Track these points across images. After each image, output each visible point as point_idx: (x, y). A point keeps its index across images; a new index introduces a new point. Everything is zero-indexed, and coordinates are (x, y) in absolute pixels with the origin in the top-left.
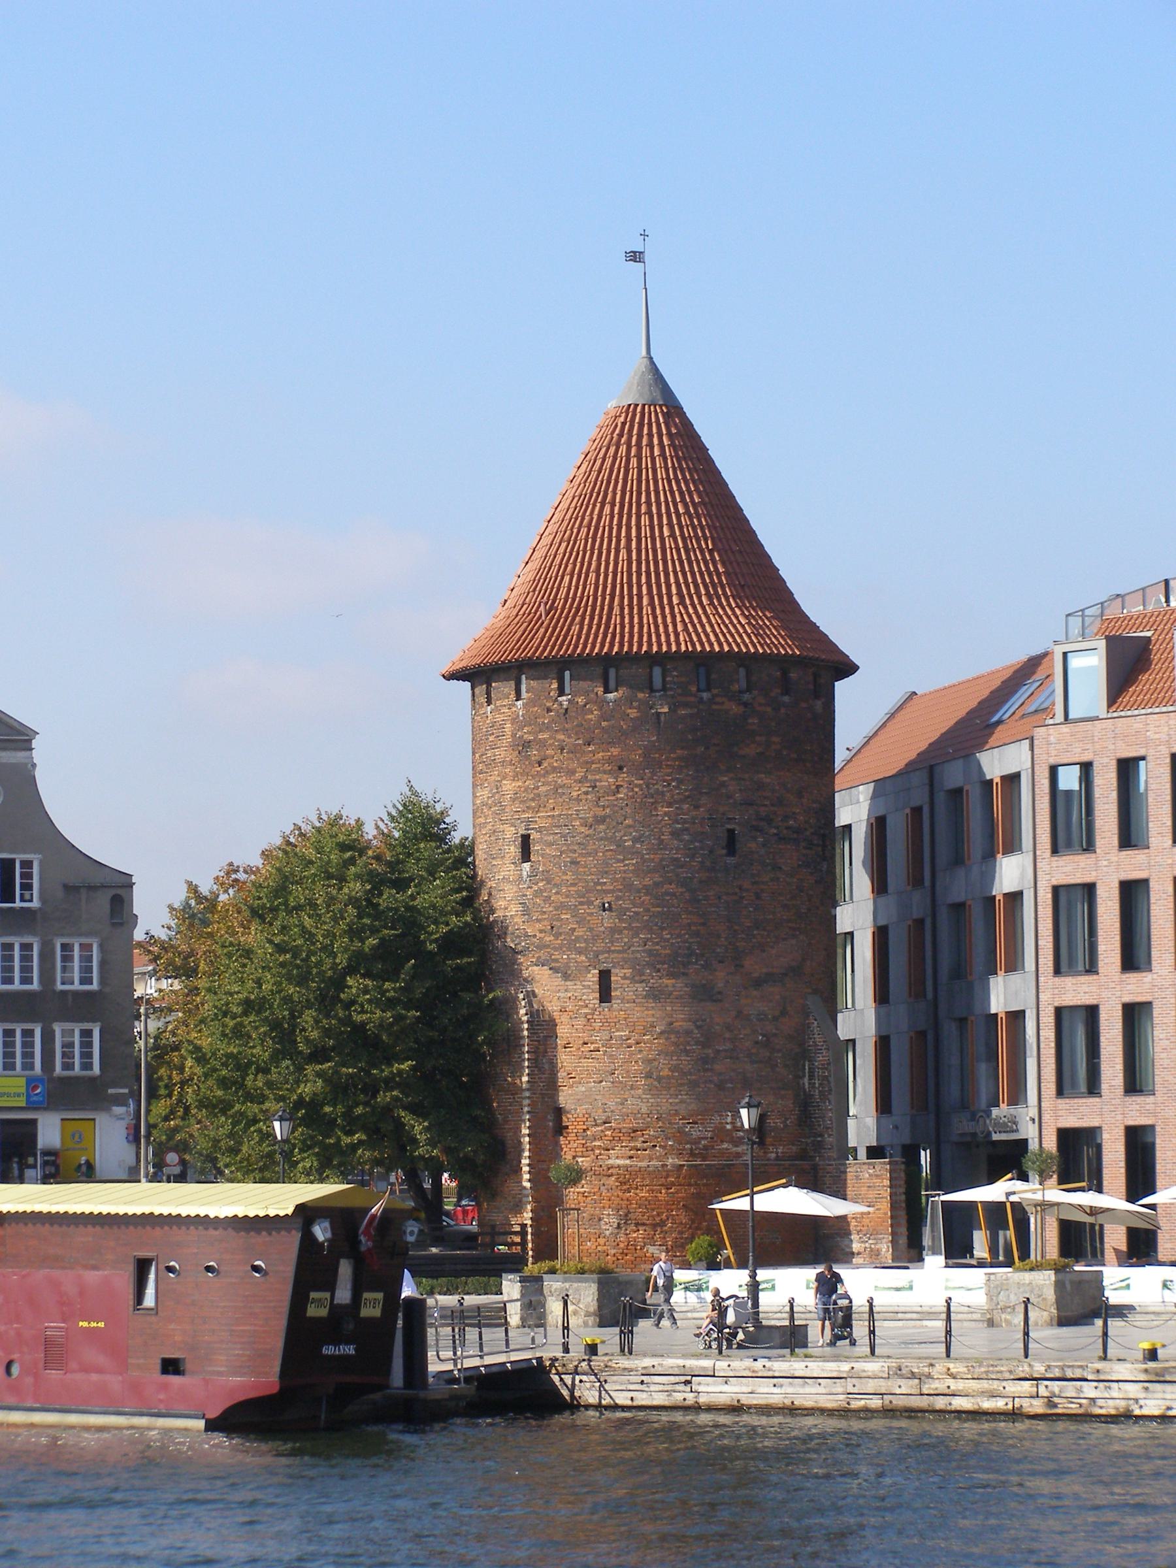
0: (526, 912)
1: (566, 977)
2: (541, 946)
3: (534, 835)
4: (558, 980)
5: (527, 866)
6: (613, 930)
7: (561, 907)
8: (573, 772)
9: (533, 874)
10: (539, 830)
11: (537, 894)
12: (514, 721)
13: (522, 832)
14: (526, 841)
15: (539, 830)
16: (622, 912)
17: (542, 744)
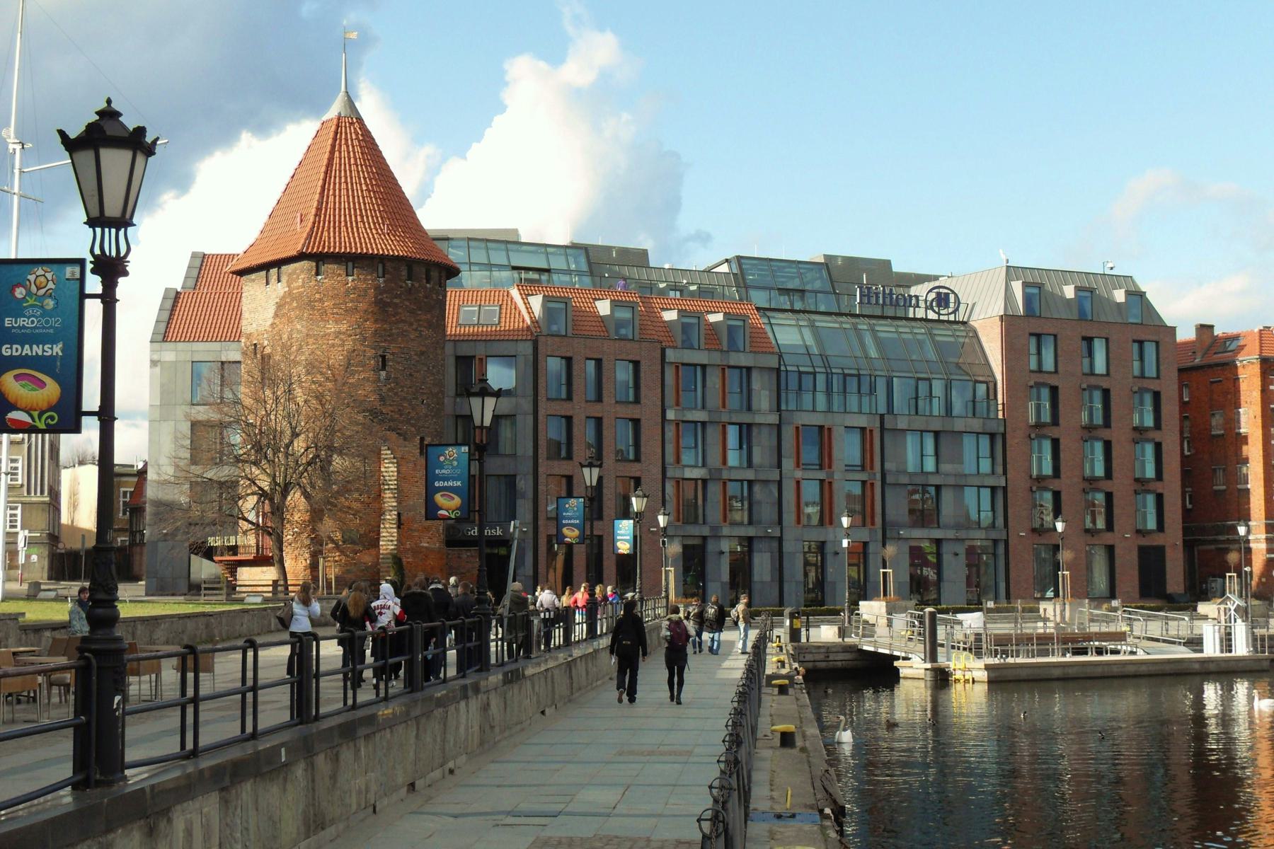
0: (382, 399)
1: (405, 439)
2: (392, 420)
3: (388, 356)
4: (401, 441)
5: (383, 373)
6: (426, 416)
7: (405, 399)
8: (411, 324)
9: (388, 378)
10: (393, 354)
11: (389, 390)
12: (377, 288)
13: (380, 353)
14: (383, 357)
15: (393, 354)
16: (428, 405)
17: (396, 305)
